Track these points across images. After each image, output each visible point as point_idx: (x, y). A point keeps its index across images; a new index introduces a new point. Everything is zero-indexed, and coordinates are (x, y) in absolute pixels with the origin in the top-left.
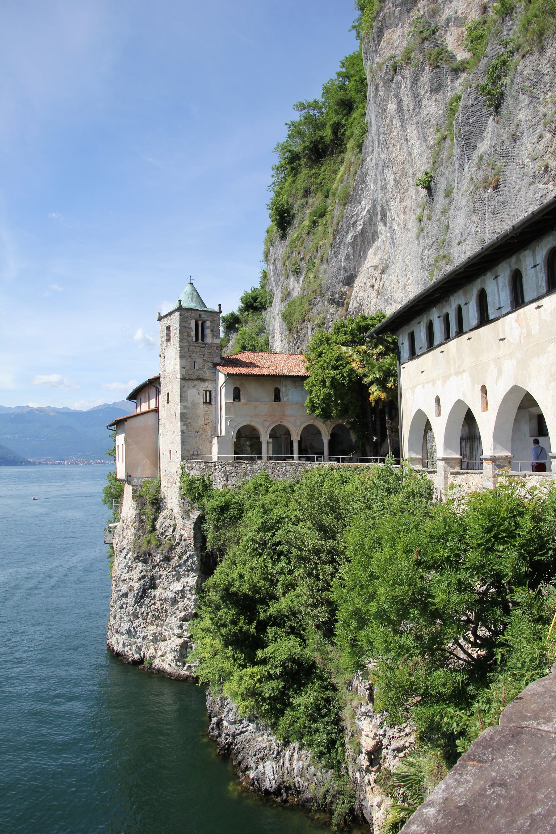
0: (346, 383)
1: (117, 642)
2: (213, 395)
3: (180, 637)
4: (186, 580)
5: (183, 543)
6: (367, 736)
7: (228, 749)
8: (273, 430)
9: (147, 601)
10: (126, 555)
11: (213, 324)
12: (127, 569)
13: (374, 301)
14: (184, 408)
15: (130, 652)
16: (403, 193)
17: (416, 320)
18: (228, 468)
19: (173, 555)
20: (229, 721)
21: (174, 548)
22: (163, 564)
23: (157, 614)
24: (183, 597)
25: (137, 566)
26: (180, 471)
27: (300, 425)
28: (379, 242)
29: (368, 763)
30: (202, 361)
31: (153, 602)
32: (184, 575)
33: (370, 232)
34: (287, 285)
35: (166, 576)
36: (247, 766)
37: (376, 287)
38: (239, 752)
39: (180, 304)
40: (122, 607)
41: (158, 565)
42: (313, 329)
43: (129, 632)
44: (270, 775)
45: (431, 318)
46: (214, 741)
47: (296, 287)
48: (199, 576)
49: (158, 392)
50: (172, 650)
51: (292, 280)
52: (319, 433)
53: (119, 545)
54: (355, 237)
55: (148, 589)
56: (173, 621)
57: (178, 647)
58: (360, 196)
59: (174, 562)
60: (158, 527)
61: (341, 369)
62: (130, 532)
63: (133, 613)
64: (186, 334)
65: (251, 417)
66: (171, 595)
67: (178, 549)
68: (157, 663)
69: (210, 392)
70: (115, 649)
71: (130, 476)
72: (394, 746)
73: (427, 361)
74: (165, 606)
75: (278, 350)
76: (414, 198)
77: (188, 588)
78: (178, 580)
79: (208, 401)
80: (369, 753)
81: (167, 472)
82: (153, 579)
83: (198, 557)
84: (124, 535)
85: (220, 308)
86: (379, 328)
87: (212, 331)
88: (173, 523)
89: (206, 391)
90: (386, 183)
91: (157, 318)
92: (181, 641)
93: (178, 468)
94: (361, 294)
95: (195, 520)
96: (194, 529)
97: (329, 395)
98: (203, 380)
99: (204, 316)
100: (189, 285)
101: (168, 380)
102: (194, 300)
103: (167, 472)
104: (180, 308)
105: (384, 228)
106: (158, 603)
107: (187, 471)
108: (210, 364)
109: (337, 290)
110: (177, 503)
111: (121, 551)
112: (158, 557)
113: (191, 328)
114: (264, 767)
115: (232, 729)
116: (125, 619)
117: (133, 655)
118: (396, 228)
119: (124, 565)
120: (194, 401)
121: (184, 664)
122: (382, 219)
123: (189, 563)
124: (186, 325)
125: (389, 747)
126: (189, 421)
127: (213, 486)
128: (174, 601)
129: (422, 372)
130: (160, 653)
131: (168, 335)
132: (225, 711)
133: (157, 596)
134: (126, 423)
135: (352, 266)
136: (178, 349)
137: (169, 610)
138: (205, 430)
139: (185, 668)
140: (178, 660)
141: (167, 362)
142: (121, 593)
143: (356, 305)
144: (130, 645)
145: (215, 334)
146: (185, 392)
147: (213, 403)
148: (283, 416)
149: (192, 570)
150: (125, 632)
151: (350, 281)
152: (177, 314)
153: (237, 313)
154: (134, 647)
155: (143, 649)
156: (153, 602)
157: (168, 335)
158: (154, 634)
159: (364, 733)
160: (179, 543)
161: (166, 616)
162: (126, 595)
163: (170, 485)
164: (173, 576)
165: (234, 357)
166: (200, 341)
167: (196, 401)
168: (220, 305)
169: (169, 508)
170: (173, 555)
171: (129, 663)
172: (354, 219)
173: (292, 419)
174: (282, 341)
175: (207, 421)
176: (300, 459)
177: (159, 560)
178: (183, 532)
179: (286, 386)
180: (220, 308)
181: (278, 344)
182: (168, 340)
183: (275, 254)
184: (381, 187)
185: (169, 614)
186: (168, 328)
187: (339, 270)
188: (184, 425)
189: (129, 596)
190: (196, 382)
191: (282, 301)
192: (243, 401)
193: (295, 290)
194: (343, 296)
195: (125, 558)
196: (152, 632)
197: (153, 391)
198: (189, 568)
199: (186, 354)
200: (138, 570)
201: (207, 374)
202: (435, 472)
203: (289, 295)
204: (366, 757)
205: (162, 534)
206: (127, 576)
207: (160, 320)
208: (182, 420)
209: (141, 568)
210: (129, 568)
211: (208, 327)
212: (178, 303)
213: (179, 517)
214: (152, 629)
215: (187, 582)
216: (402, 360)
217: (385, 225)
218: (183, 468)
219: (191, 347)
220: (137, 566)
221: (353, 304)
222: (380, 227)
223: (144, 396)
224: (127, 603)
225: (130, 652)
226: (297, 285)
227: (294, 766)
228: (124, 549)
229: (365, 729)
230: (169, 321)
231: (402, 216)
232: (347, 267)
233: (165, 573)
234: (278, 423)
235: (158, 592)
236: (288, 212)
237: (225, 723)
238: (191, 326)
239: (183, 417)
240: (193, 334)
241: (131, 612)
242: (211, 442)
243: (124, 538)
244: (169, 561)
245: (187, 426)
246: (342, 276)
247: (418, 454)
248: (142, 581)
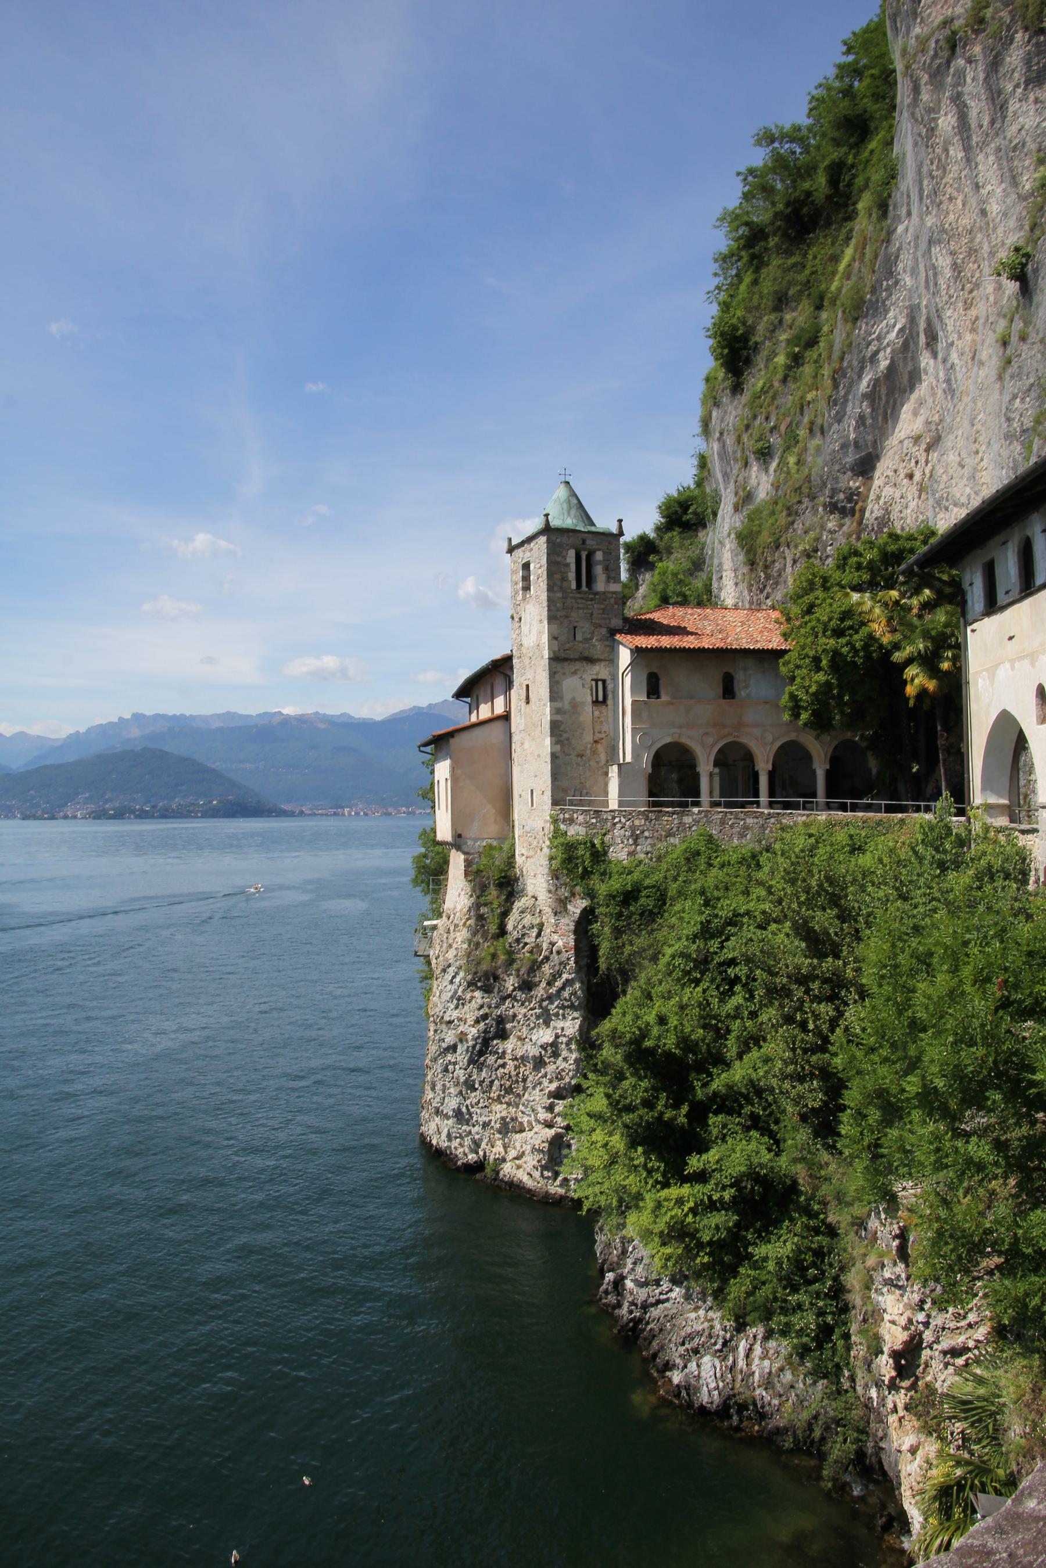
0: (859, 661)
1: (437, 1130)
2: (610, 687)
3: (549, 1125)
4: (560, 1024)
5: (555, 957)
6: (893, 1322)
7: (634, 1329)
8: (720, 751)
9: (491, 1059)
10: (454, 977)
12: (455, 1001)
13: (912, 505)
14: (556, 711)
15: (461, 1150)
16: (971, 292)
17: (999, 538)
18: (637, 823)
19: (537, 979)
20: (635, 1281)
21: (539, 967)
22: (519, 994)
23: (508, 1083)
24: (556, 1055)
25: (472, 997)
26: (549, 828)
27: (772, 743)
28: (922, 390)
29: (893, 1373)
30: (588, 625)
31: (500, 1062)
32: (557, 1015)
33: (904, 370)
34: (746, 480)
35: (525, 1016)
36: (668, 1362)
37: (917, 477)
38: (654, 1336)
39: (547, 521)
40: (446, 1070)
41: (509, 996)
42: (795, 562)
43: (458, 1114)
44: (709, 1380)
45: (1029, 533)
46: (608, 1313)
47: (762, 483)
48: (585, 1019)
49: (509, 684)
50: (534, 1149)
51: (755, 469)
52: (807, 757)
53: (441, 958)
54: (876, 383)
55: (493, 1039)
56: (537, 1097)
57: (546, 1145)
58: (884, 302)
59: (540, 991)
60: (510, 927)
61: (851, 636)
62: (461, 936)
63: (466, 1081)
64: (558, 576)
65: (680, 727)
66: (534, 1051)
67: (547, 969)
68: (507, 1170)
69: (604, 682)
70: (434, 1142)
71: (460, 836)
72: (945, 1344)
73: (1020, 616)
74: (522, 1070)
75: (729, 602)
76: (992, 299)
77: (565, 1040)
78: (547, 1024)
79: (601, 698)
80: (896, 1355)
81: (527, 828)
82: (501, 1020)
83: (582, 983)
84: (451, 941)
86: (925, 554)
87: (606, 569)
88: (538, 921)
89: (597, 681)
90: (935, 275)
91: (505, 546)
92: (552, 1132)
93: (546, 821)
94: (888, 491)
95: (577, 916)
96: (575, 932)
97: (828, 684)
98: (590, 660)
100: (562, 486)
101: (527, 661)
102: (573, 512)
103: (527, 828)
104: (547, 530)
105: (932, 362)
106: (511, 1065)
107: (562, 827)
108: (604, 631)
109: (842, 485)
110: (545, 885)
111: (444, 971)
112: (510, 983)
113: (568, 565)
114: (698, 1366)
115: (642, 1294)
116: (452, 1090)
117: (465, 1154)
118: (956, 361)
119: (450, 994)
120: (574, 699)
121: (556, 1174)
122: (928, 345)
123: (565, 994)
124: (559, 559)
125: (935, 1346)
126: (565, 735)
127: (610, 854)
128: (539, 1063)
129: (1011, 638)
130: (512, 1153)
131: (526, 579)
132: (629, 1262)
133: (509, 1051)
134: (452, 740)
135: (870, 438)
136: (545, 604)
137: (530, 1078)
138: (594, 752)
139: (558, 1182)
140: (544, 1168)
141: (525, 629)
142: (444, 1045)
143: (877, 513)
144: (461, 1137)
145: (613, 574)
146: (558, 682)
147: (610, 702)
148: (740, 725)
149: (572, 1007)
150: (451, 1113)
151: (865, 467)
152: (543, 539)
153: (652, 535)
154: (467, 1141)
155: (483, 1145)
156: (500, 1062)
157: (526, 579)
158: (503, 1119)
159: (887, 1317)
160: (547, 958)
161: (525, 1089)
162: (453, 1048)
163: (531, 853)
164: (538, 1017)
165: (648, 616)
166: (584, 588)
167: (578, 699)
168: (620, 521)
169: (530, 894)
170: (537, 979)
171: (458, 1169)
172: (872, 348)
173: (757, 732)
174: (736, 584)
175: (598, 736)
176: (771, 805)
177: (511, 988)
178: (555, 937)
179: (745, 669)
180: (620, 527)
181: (729, 591)
182: (526, 588)
183: (722, 421)
184: (927, 281)
185: (529, 1084)
186: (526, 566)
187: (844, 446)
188: (557, 743)
189: (459, 1051)
190: (578, 665)
191: (736, 509)
192: (664, 698)
193: (761, 488)
194: (852, 496)
195: (451, 982)
196: (498, 1116)
197: (499, 683)
198: (566, 1004)
199: (559, 614)
200: (474, 1005)
201: (598, 648)
202: (1034, 831)
203: (749, 497)
204: (891, 1361)
205: (518, 941)
206: (455, 1014)
207: (511, 550)
208: (551, 736)
209: (480, 1001)
210: (459, 999)
211: (599, 563)
212: (543, 519)
213: (547, 910)
214: (499, 1110)
215: (563, 1029)
216: (970, 617)
217: (935, 355)
218: (555, 821)
220: (472, 997)
221: (873, 511)
222: (925, 360)
223: (483, 691)
224: (455, 1063)
225: (461, 1150)
226: (764, 478)
227: (754, 1368)
228: (449, 966)
229: (889, 1310)
230: (528, 554)
231: (968, 337)
232: (861, 442)
233: (523, 1011)
234: (730, 739)
235: (509, 1045)
236: (745, 338)
237: (629, 1284)
238: (568, 560)
239: (556, 728)
240: (572, 575)
241: (462, 1079)
242: (607, 774)
243: (450, 946)
244: (530, 990)
245: (563, 745)
246: (850, 459)
247: (999, 795)
248: (482, 1026)
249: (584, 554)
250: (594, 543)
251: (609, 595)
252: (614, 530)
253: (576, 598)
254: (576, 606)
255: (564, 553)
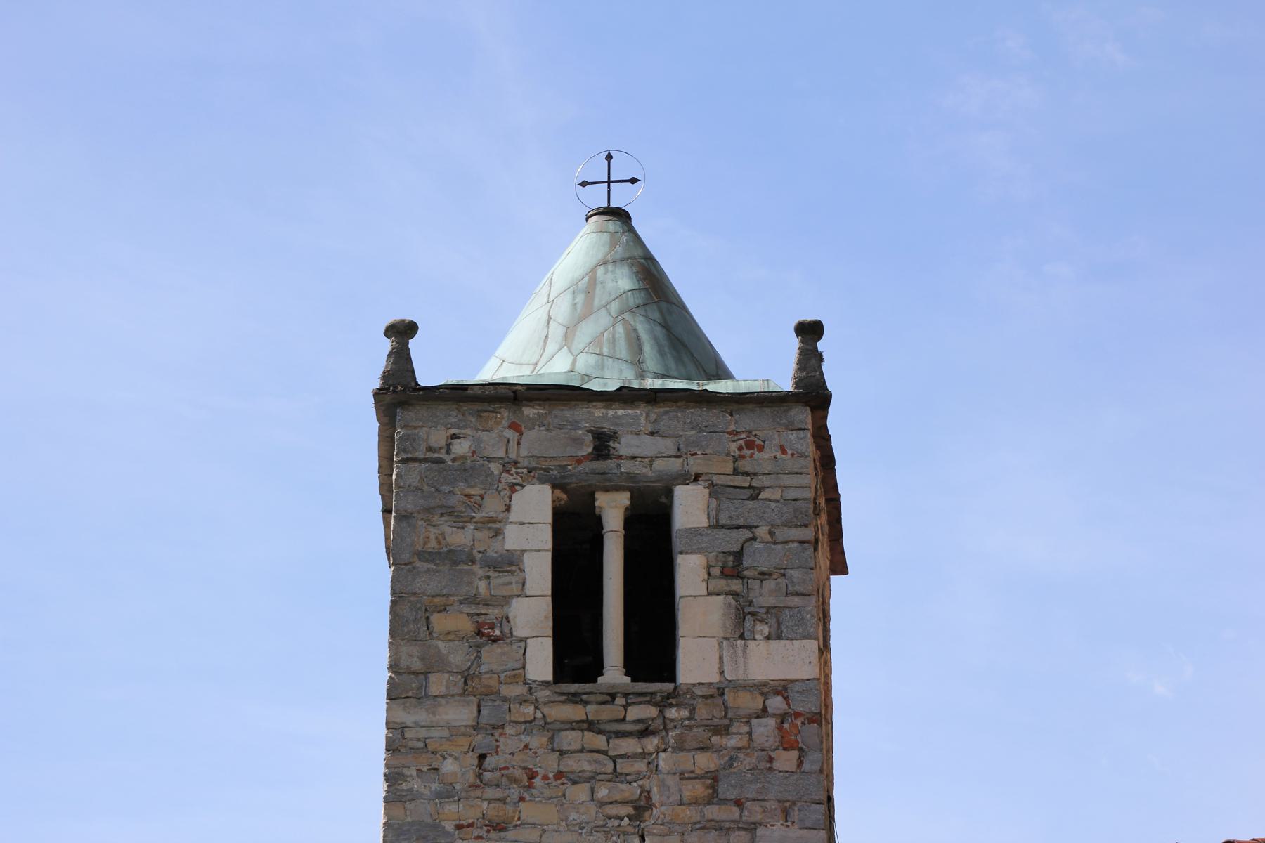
11: (735, 511)
85: (810, 360)
87: (732, 568)
99: (643, 446)
113: (510, 563)
124: (460, 538)
145: (765, 595)
168: (810, 331)
180: (810, 360)
219: (510, 741)
238: (513, 539)
240: (532, 614)
249: (613, 511)
250: (649, 446)
251: (749, 702)
252: (784, 382)
253: (551, 728)
254: (550, 764)
255: (492, 507)
